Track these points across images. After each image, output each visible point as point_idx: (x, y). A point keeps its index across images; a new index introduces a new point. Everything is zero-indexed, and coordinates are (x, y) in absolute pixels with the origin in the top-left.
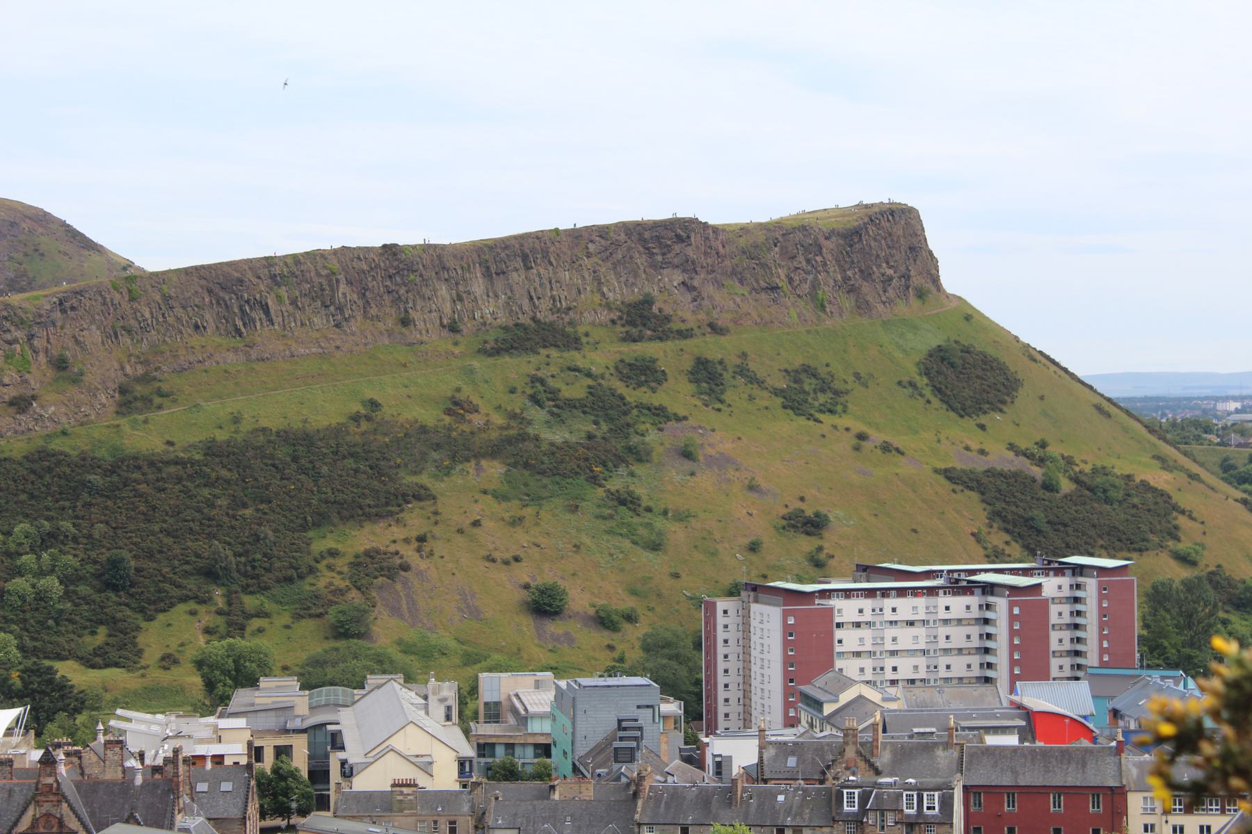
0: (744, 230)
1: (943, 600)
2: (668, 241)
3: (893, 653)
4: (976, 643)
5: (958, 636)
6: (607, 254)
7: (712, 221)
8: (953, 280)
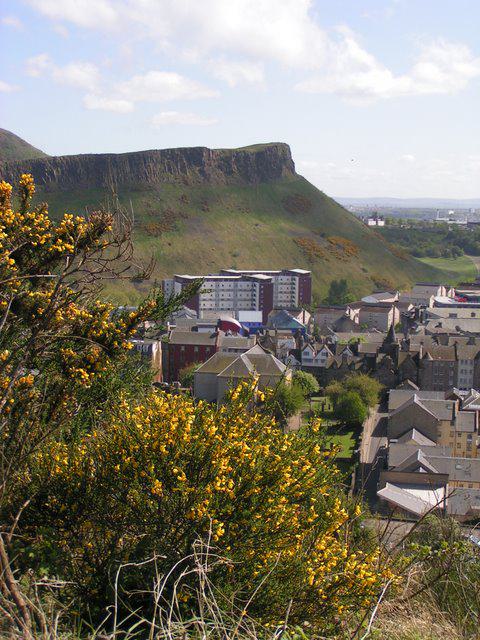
0: (223, 151)
1: (239, 283)
2: (194, 157)
3: (222, 300)
4: (250, 297)
5: (244, 295)
6: (172, 158)
7: (212, 148)
8: (299, 170)
